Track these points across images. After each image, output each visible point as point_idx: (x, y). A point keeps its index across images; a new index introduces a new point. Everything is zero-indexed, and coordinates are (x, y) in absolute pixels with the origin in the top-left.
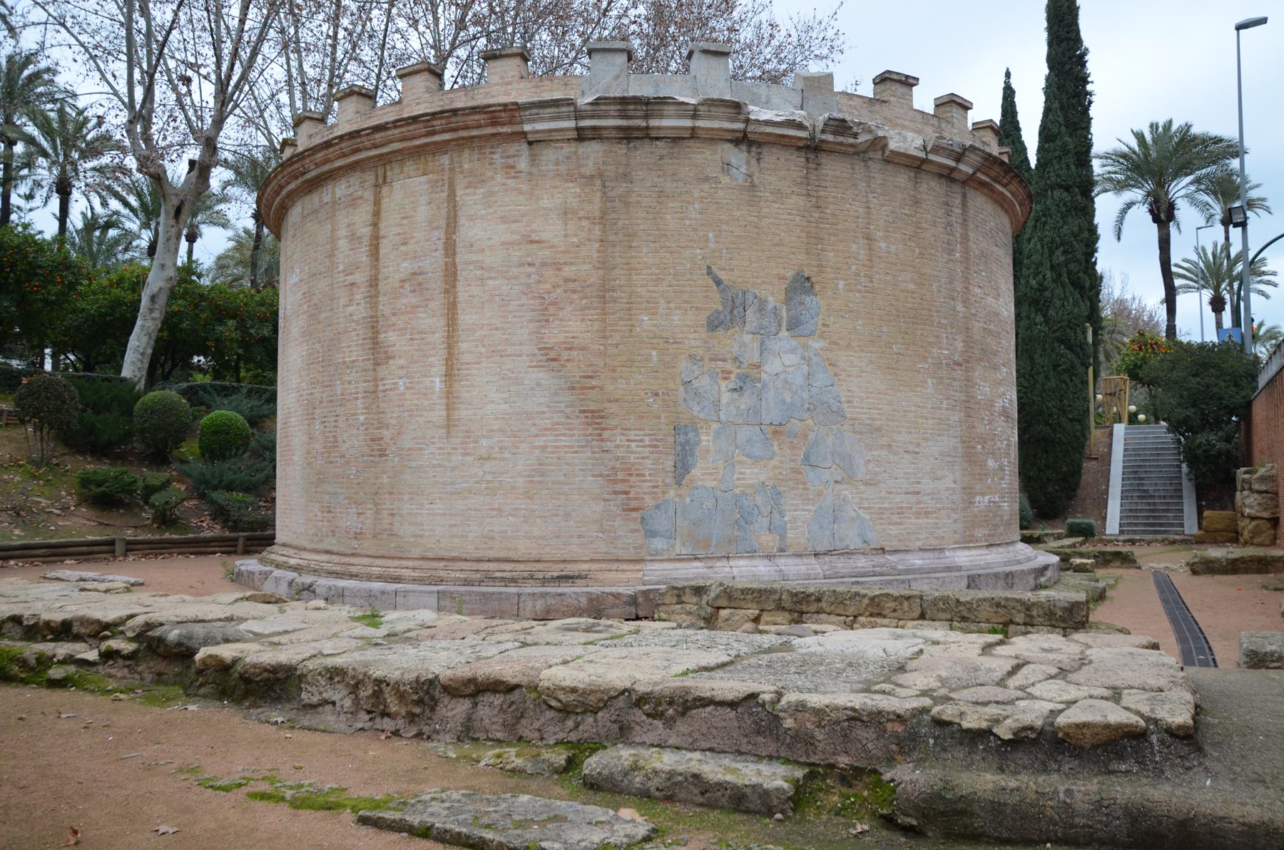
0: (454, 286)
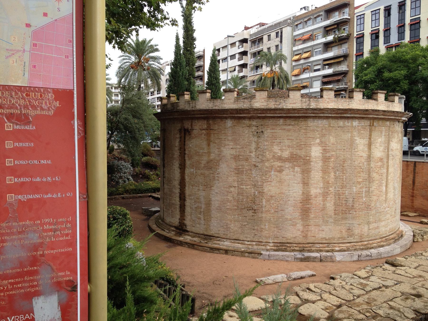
0: (388, 161)
